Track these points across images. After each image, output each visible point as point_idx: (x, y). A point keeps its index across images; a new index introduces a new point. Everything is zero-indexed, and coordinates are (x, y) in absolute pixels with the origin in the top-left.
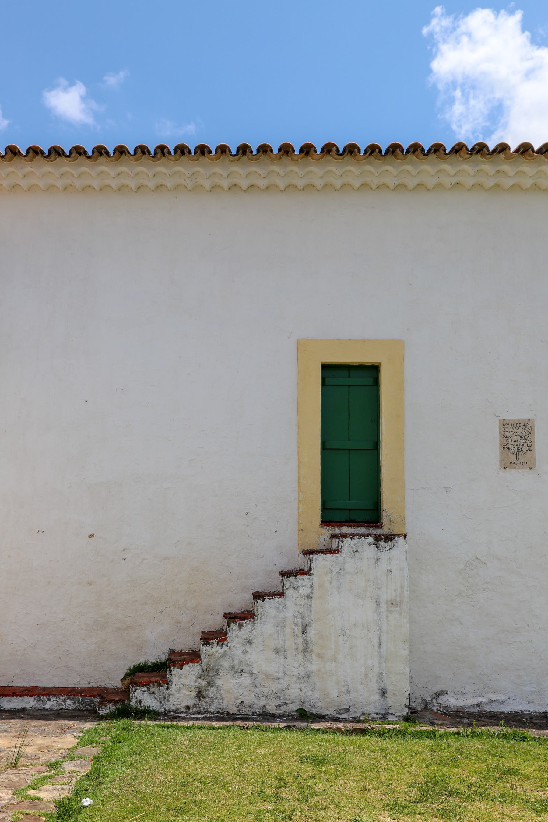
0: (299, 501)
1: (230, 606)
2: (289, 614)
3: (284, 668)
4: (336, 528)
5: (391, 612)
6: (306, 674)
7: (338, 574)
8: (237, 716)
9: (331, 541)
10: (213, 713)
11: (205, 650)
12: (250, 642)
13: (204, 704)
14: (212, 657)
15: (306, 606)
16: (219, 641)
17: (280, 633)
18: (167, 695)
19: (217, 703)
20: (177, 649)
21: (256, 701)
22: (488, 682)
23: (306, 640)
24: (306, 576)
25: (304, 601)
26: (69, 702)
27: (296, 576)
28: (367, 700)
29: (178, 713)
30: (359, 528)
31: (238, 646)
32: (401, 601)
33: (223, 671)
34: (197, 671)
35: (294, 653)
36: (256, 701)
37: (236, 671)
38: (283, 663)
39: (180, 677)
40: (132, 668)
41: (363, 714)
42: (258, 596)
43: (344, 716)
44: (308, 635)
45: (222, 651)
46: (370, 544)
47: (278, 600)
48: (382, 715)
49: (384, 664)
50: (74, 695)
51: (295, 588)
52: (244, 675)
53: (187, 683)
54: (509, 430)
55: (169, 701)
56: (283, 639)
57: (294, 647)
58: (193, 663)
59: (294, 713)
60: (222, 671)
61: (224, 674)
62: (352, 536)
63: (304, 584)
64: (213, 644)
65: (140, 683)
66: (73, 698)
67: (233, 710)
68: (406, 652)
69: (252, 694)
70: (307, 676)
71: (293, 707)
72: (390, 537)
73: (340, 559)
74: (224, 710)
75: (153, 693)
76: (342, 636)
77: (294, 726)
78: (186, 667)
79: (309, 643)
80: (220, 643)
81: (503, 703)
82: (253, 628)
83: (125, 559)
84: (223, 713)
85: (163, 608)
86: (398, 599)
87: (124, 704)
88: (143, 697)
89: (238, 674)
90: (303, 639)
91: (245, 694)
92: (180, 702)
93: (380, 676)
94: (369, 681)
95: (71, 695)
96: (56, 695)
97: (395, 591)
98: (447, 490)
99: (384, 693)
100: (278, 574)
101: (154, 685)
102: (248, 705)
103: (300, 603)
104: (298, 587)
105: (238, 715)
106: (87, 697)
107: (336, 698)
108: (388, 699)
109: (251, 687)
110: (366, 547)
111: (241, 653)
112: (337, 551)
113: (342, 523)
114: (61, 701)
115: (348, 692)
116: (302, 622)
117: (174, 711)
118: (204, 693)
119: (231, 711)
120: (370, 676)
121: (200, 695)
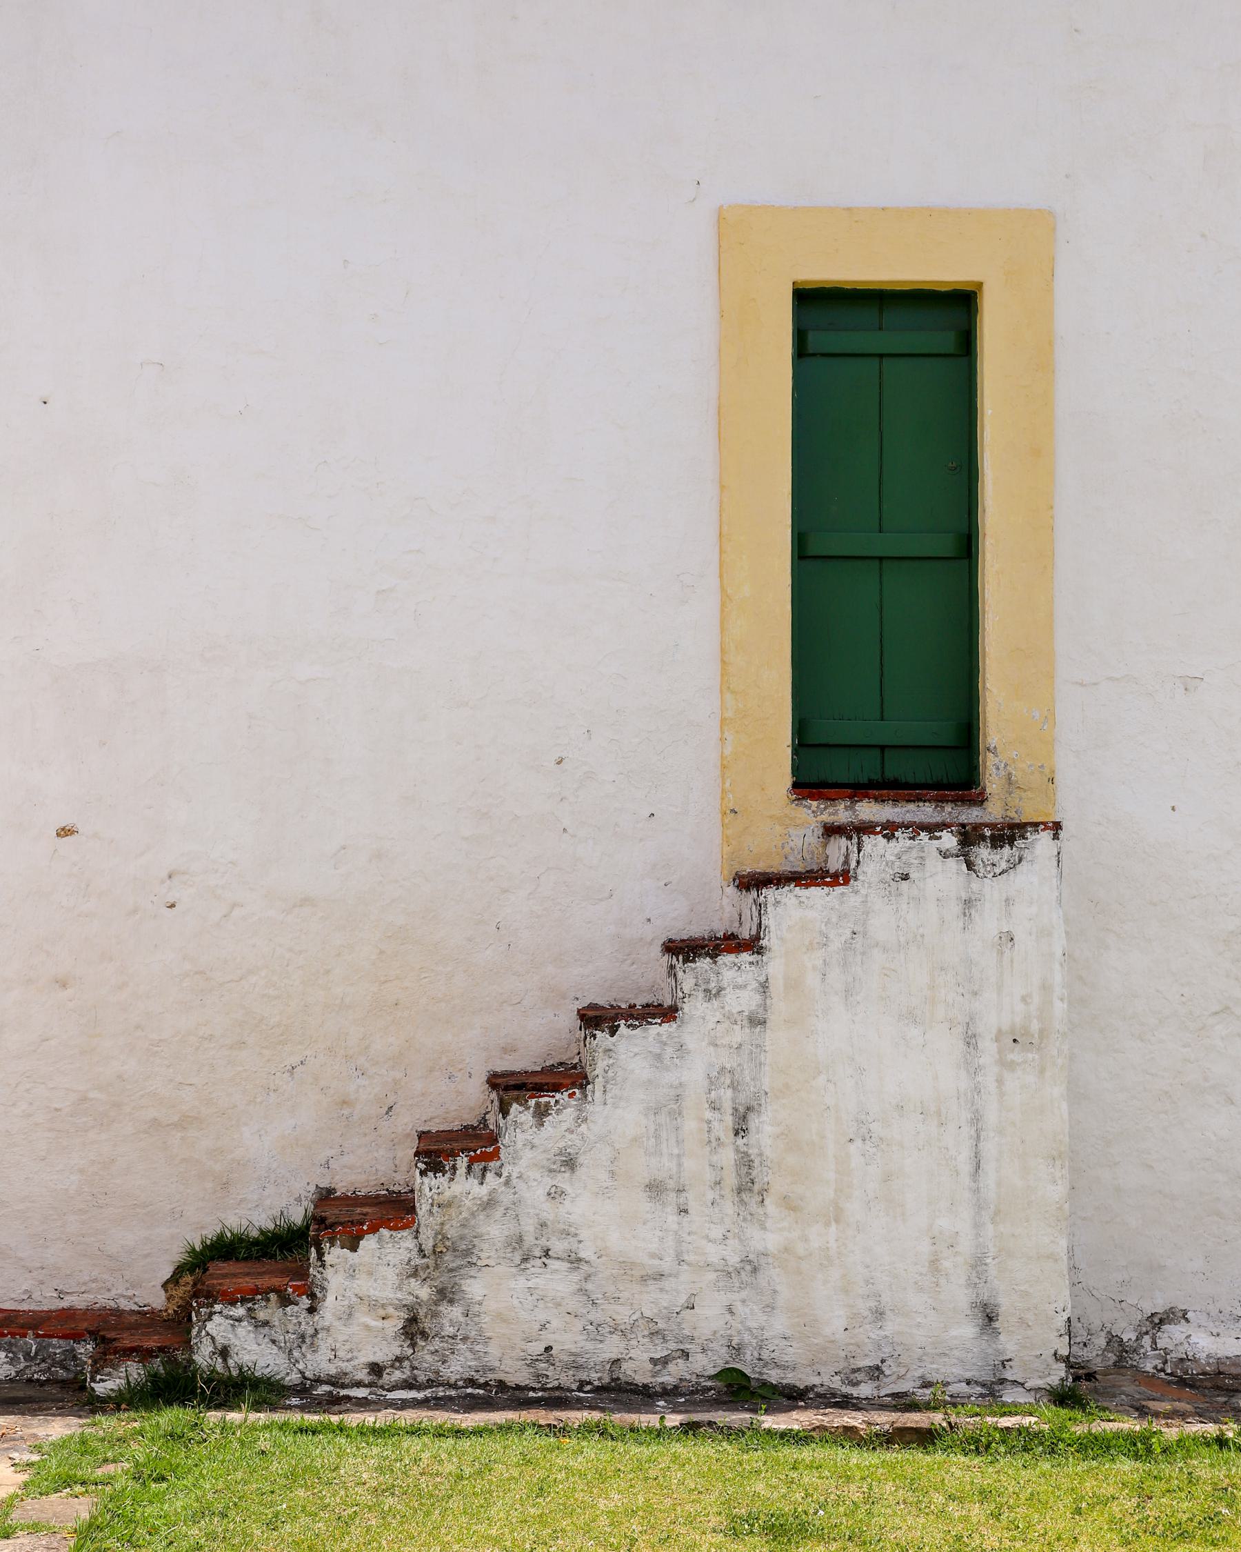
1: (508, 1050)
2: (694, 1074)
3: (680, 1241)
4: (841, 806)
5: (1011, 1066)
7: (848, 947)
8: (531, 1394)
9: (825, 846)
10: (454, 1386)
11: (429, 1188)
12: (570, 1163)
13: (426, 1357)
14: (453, 1211)
15: (746, 1048)
16: (472, 1161)
17: (664, 1135)
18: (310, 1331)
19: (468, 1354)
20: (342, 1186)
21: (589, 1346)
23: (746, 1154)
24: (746, 957)
25: (739, 1034)
27: (714, 957)
28: (935, 1341)
29: (343, 1386)
30: (911, 806)
31: (534, 1174)
32: (1041, 1031)
33: (486, 1253)
34: (405, 1256)
35: (710, 1195)
36: (589, 1346)
37: (528, 1254)
38: (675, 1227)
39: (352, 1273)
42: (596, 1019)
43: (865, 1390)
44: (752, 1138)
45: (482, 1191)
46: (945, 855)
47: (657, 1030)
48: (983, 1385)
49: (990, 1227)
50: (13, 1335)
51: (713, 994)
53: (372, 1292)
55: (314, 1348)
56: (676, 1151)
57: (709, 1176)
58: (391, 1229)
59: (709, 1384)
60: (483, 1255)
61: (491, 1262)
62: (890, 830)
63: (740, 981)
64: (454, 1168)
65: (224, 1293)
67: (517, 1375)
68: (1056, 1192)
69: (578, 1325)
70: (748, 1268)
71: (705, 1364)
72: (1008, 834)
74: (490, 1376)
76: (858, 1142)
77: (710, 1424)
78: (368, 1243)
79: (756, 1164)
80: (477, 1167)
82: (581, 1119)
83: (172, 906)
84: (486, 1384)
85: (294, 1060)
86: (1035, 1026)
87: (171, 1362)
88: (234, 1337)
89: (532, 1262)
90: (737, 1151)
91: (555, 1323)
92: (351, 1351)
93: (978, 1264)
94: (943, 1281)
97: (1025, 999)
98: (1189, 684)
99: (989, 1317)
100: (657, 949)
101: (268, 1300)
102: (566, 1358)
103: (725, 1041)
104: (720, 990)
105: (534, 1389)
106: (54, 1341)
107: (841, 1336)
108: (1001, 1337)
109: (573, 1304)
110: (934, 862)
111: (543, 1198)
112: (843, 877)
113: (858, 790)
115: (879, 1314)
116: (733, 1100)
117: (334, 1381)
118: (427, 1324)
119: (511, 1380)
120: (946, 1264)
121: (413, 1330)
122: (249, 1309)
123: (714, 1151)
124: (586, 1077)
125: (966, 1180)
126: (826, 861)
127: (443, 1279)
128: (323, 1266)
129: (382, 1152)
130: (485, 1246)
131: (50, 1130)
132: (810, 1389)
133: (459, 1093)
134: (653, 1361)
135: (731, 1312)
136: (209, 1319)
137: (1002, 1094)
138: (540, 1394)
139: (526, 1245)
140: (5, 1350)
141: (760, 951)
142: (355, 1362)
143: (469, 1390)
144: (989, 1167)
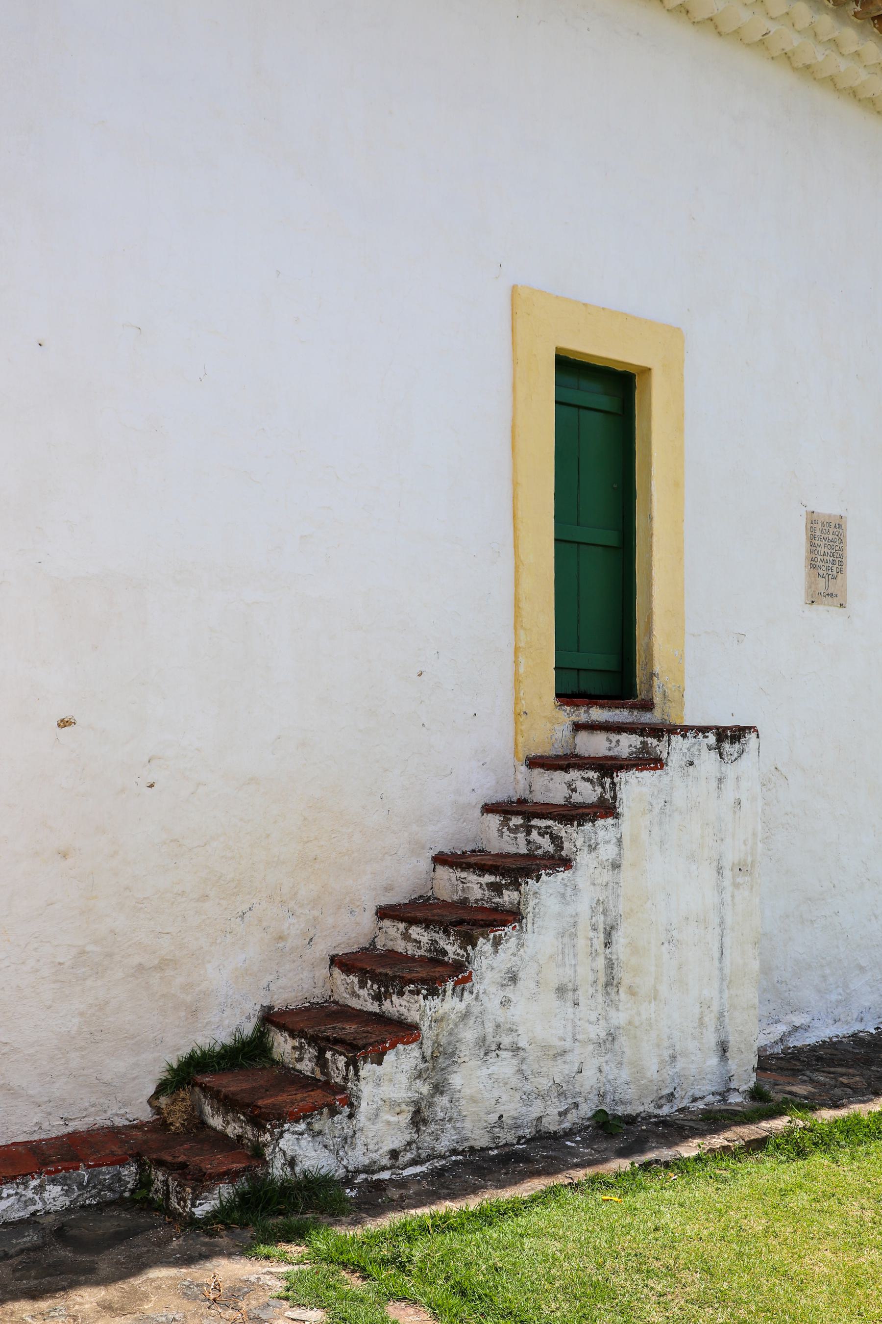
0: (517, 650)
1: (388, 889)
2: (583, 906)
3: (574, 1026)
6: (610, 1034)
7: (662, 812)
9: (574, 737)
10: (442, 1157)
12: (513, 979)
13: (426, 1139)
14: (444, 1024)
15: (611, 884)
16: (456, 984)
17: (566, 951)
18: (351, 1133)
19: (452, 1131)
21: (524, 1110)
22: (787, 994)
23: (611, 959)
25: (607, 876)
26: (54, 1191)
27: (593, 821)
29: (373, 1172)
30: (617, 711)
31: (492, 989)
32: (752, 862)
33: (464, 1052)
34: (413, 1062)
35: (591, 990)
37: (488, 1049)
38: (572, 1016)
40: (175, 1066)
41: (695, 1100)
44: (614, 947)
45: (461, 1007)
46: (710, 748)
48: (720, 1094)
49: (727, 991)
50: (67, 1169)
51: (593, 848)
52: (504, 1054)
54: (818, 533)
55: (353, 1146)
56: (573, 963)
57: (591, 977)
58: (404, 1043)
59: (588, 1123)
60: (462, 1054)
61: (466, 1059)
63: (607, 838)
64: (445, 991)
65: (292, 1114)
66: (65, 1178)
68: (755, 965)
69: (518, 1095)
70: (610, 1038)
71: (587, 1110)
73: (666, 779)
74: (466, 1144)
75: (320, 1133)
76: (666, 944)
77: (657, 1161)
78: (390, 1057)
79: (615, 966)
80: (459, 988)
81: (806, 1028)
83: (151, 786)
84: (463, 1150)
85: (245, 908)
86: (749, 860)
87: (253, 1178)
89: (490, 1055)
90: (606, 958)
92: (377, 1143)
93: (721, 1016)
94: (704, 1031)
95: (58, 1171)
96: (15, 1178)
97: (745, 843)
101: (321, 1114)
102: (510, 1122)
104: (597, 844)
105: (491, 1149)
106: (104, 1169)
107: (656, 1077)
108: (729, 1062)
109: (515, 1081)
111: (498, 1006)
114: (30, 1194)
115: (673, 1058)
116: (604, 922)
118: (426, 1113)
120: (706, 1019)
121: (418, 1120)
122: (309, 1124)
123: (593, 960)
124: (520, 914)
125: (716, 962)
126: (575, 748)
127: (436, 1077)
128: (358, 1080)
129: (305, 974)
130: (463, 1048)
131: (55, 982)
132: (638, 1115)
133: (358, 923)
134: (560, 1114)
135: (600, 1071)
136: (281, 1136)
137: (734, 905)
138: (496, 1152)
139: (487, 1042)
140: (61, 1184)
141: (617, 816)
142: (381, 1152)
143: (454, 1158)
144: (727, 952)
